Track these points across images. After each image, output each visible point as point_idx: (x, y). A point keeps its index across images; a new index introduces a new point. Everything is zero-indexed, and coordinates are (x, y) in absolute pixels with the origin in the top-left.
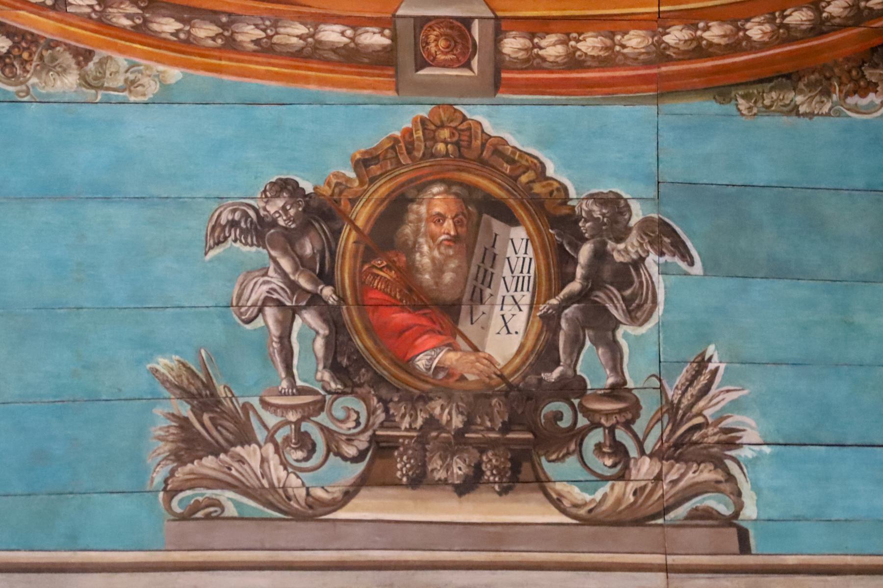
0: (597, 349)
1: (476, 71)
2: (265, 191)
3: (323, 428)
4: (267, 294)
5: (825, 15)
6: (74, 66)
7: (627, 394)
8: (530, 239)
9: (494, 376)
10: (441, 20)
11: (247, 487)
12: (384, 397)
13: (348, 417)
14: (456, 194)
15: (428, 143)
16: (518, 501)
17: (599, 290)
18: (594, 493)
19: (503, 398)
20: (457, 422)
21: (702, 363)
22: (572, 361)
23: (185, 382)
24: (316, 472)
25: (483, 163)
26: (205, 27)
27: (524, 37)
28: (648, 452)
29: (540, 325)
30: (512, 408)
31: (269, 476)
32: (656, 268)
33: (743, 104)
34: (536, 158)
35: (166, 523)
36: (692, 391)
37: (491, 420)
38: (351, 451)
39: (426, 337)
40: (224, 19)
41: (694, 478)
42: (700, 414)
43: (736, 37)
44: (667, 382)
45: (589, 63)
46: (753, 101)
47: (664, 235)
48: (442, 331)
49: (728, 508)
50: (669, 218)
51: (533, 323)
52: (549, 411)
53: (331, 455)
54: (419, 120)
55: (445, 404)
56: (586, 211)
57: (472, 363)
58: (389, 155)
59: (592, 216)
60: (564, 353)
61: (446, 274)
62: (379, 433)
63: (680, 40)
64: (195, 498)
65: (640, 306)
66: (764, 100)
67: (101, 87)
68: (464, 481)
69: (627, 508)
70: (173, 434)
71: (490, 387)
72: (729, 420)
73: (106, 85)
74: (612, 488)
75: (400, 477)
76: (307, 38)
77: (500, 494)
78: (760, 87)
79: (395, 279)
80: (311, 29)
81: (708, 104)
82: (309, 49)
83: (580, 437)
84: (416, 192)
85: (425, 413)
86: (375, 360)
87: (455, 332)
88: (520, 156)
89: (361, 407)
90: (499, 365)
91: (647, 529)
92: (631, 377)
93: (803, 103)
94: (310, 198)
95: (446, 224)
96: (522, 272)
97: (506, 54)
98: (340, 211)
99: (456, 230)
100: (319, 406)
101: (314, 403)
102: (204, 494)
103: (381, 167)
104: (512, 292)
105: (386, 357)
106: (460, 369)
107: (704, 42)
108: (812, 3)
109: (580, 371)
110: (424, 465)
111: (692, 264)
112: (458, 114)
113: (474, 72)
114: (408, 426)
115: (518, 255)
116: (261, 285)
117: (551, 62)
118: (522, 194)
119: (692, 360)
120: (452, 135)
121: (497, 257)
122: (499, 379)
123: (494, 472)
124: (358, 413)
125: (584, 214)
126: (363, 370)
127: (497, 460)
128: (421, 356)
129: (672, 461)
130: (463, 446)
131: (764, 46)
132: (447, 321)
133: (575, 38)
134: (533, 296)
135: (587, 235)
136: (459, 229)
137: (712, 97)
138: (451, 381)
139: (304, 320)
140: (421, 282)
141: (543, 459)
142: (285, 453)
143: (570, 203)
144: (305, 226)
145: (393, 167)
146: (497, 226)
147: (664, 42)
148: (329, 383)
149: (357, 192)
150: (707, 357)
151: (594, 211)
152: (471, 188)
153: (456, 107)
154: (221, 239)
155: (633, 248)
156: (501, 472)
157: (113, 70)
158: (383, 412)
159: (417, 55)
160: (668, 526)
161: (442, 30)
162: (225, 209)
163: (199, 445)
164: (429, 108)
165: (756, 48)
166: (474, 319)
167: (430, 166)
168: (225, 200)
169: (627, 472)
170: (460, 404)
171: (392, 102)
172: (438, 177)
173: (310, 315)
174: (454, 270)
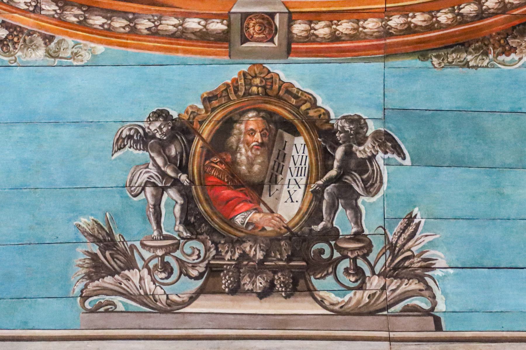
1: (277, 43)
3: (177, 259)
8: (306, 144)
9: (283, 228)
10: (257, 14)
13: (193, 253)
14: (262, 117)
15: (247, 87)
20: (260, 255)
21: (410, 219)
24: (172, 285)
25: (278, 97)
27: (306, 23)
33: (435, 61)
36: (405, 236)
37: (280, 254)
38: (194, 273)
39: (242, 204)
48: (252, 201)
55: (253, 244)
57: (270, 220)
61: (255, 166)
62: (212, 262)
65: (372, 185)
71: (282, 235)
75: (224, 288)
84: (239, 117)
85: (240, 250)
86: (210, 217)
87: (260, 201)
88: (302, 94)
89: (201, 247)
90: (286, 221)
95: (256, 136)
96: (301, 165)
97: (294, 34)
99: (262, 139)
102: (103, 298)
104: (294, 177)
106: (262, 224)
110: (239, 282)
111: (404, 158)
112: (265, 69)
113: (275, 44)
114: (229, 258)
115: (299, 154)
120: (261, 82)
121: (286, 155)
122: (286, 230)
124: (199, 250)
128: (239, 216)
131: (448, 26)
132: (255, 195)
136: (264, 139)
138: (257, 230)
140: (240, 171)
142: (154, 274)
146: (287, 136)
152: (271, 114)
153: (264, 65)
158: (215, 249)
164: (249, 66)
166: (271, 193)
167: (247, 101)
170: (262, 244)
172: (252, 107)
174: (260, 164)
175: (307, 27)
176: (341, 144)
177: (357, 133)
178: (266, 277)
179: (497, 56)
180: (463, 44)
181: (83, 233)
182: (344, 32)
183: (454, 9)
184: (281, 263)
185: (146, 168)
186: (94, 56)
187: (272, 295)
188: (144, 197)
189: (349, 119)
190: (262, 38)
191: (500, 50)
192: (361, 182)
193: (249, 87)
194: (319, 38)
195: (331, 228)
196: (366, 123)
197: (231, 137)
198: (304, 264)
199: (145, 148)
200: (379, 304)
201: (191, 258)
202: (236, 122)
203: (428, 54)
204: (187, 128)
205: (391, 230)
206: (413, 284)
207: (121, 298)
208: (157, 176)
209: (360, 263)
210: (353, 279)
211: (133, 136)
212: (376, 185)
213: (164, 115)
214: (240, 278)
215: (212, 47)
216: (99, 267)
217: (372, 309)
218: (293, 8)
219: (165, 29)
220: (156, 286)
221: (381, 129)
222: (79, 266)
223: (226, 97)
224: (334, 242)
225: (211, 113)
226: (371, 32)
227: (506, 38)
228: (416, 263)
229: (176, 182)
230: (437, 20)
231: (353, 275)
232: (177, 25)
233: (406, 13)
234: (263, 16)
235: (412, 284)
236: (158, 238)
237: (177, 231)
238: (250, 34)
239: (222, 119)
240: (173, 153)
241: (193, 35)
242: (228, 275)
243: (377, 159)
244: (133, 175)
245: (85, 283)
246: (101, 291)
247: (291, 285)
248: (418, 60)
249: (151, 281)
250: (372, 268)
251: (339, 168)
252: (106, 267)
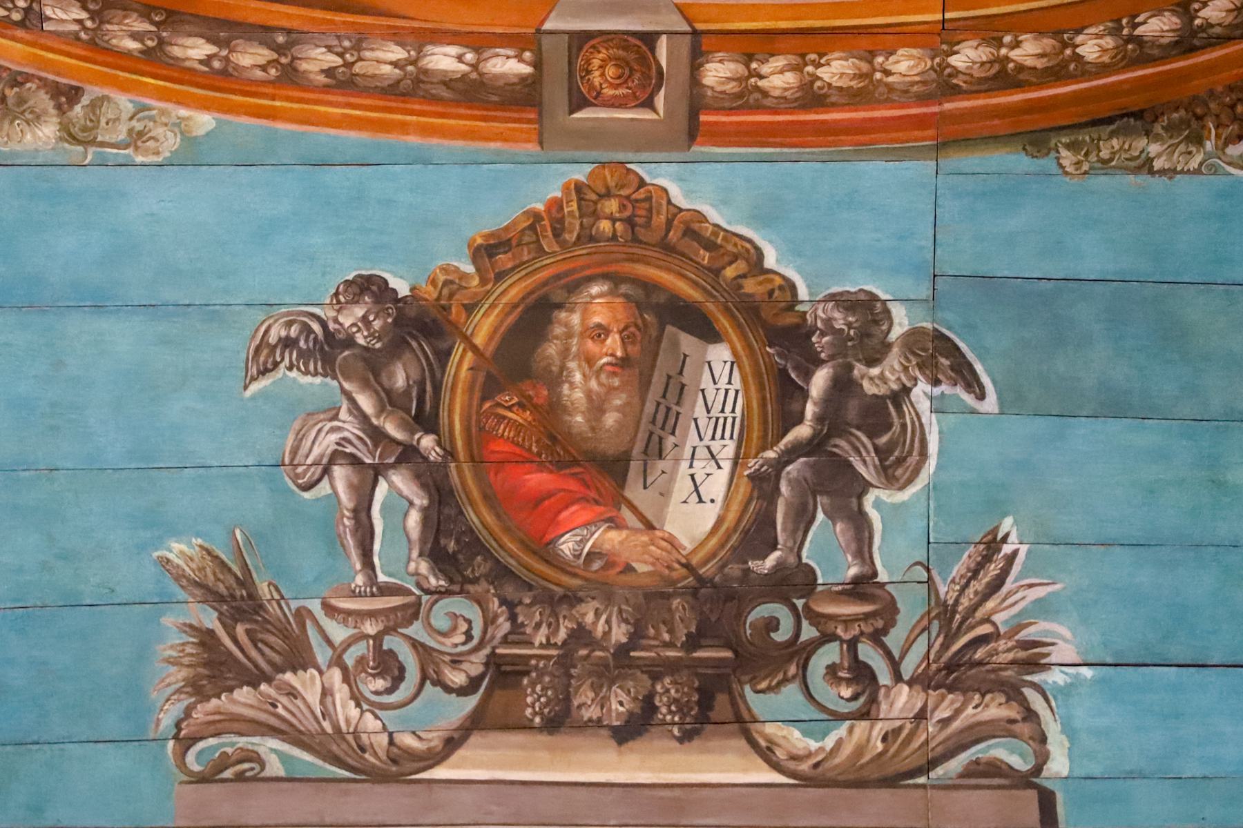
0: (834, 525)
1: (661, 113)
2: (336, 294)
3: (415, 644)
4: (336, 447)
5: (1197, 22)
6: (53, 111)
7: (878, 592)
8: (736, 362)
9: (677, 566)
10: (610, 37)
11: (300, 732)
12: (509, 598)
13: (454, 628)
14: (626, 296)
16: (709, 751)
17: (840, 436)
18: (823, 739)
19: (689, 598)
20: (619, 634)
22: (795, 543)
23: (211, 578)
24: (402, 710)
25: (668, 248)
26: (252, 51)
27: (737, 61)
28: (906, 677)
29: (749, 490)
30: (702, 613)
31: (334, 717)
32: (928, 403)
34: (750, 241)
35: (176, 784)
37: (671, 631)
39: (574, 508)
40: (281, 39)
41: (974, 715)
42: (987, 620)
43: (1061, 57)
44: (939, 574)
45: (833, 99)
46: (1083, 153)
47: (940, 354)
49: (1025, 762)
50: (949, 328)
51: (737, 486)
52: (758, 617)
53: (428, 682)
54: (573, 186)
55: (602, 607)
56: (822, 320)
57: (645, 545)
58: (526, 239)
59: (833, 327)
60: (784, 530)
61: (607, 415)
62: (498, 651)
63: (974, 63)
64: (222, 750)
66: (1100, 151)
67: (93, 142)
68: (627, 722)
69: (872, 760)
70: (192, 655)
71: (673, 583)
72: (1032, 629)
73: (100, 138)
74: (851, 730)
75: (530, 717)
76: (406, 65)
77: (681, 740)
78: (1095, 133)
79: (530, 422)
80: (412, 53)
81: (1013, 157)
82: (409, 82)
83: (804, 656)
87: (619, 500)
88: (725, 239)
89: (474, 613)
91: (900, 791)
92: (884, 566)
93: (1159, 155)
94: (405, 303)
95: (609, 341)
96: (723, 411)
97: (708, 87)
98: (450, 322)
100: (410, 611)
101: (403, 607)
103: (514, 257)
104: (707, 441)
105: (514, 539)
106: (625, 556)
107: (1011, 65)
108: (1178, 5)
109: (807, 557)
110: (568, 699)
112: (632, 176)
113: (658, 114)
114: (544, 641)
115: (717, 386)
116: (327, 433)
117: (776, 98)
118: (726, 295)
119: (977, 541)
120: (622, 207)
122: (684, 571)
123: (673, 708)
124: (469, 622)
125: (819, 324)
126: (479, 558)
127: (677, 691)
128: (567, 536)
129: (943, 691)
130: (627, 670)
132: (607, 484)
133: (814, 61)
134: (739, 447)
135: (823, 355)
136: (630, 348)
137: (1020, 148)
138: (613, 572)
139: (391, 485)
140: (570, 427)
141: (747, 689)
143: (799, 308)
144: (396, 345)
145: (531, 257)
146: (688, 342)
147: (949, 65)
148: (427, 578)
149: (476, 294)
150: (1000, 536)
151: (835, 319)
152: (649, 287)
153: (629, 166)
154: (269, 366)
155: (893, 374)
156: (682, 709)
157: (111, 116)
159: (573, 91)
160: (934, 787)
161: (611, 51)
162: (276, 321)
163: (230, 671)
165: (1090, 73)
166: (649, 482)
167: (587, 254)
168: (275, 307)
169: (874, 707)
170: (624, 607)
171: (532, 160)
173: (400, 478)
174: (618, 409)
175: (740, 69)
176: (823, 362)
177: (864, 335)
178: (635, 687)
179: (1226, 144)
181: (177, 579)
182: (834, 84)
183: (1121, 25)
184: (671, 653)
185: (331, 420)
187: (647, 735)
188: (330, 491)
189: (844, 302)
190: (625, 96)
192: (873, 454)
193: (591, 220)
194: (770, 99)
195: (797, 567)
196: (887, 312)
197: (546, 345)
198: (728, 654)
199: (329, 369)
200: (906, 758)
201: (448, 641)
202: (559, 306)
203: (1049, 140)
204: (434, 321)
205: (944, 571)
206: (993, 705)
207: (274, 743)
208: (360, 438)
209: (867, 653)
210: (847, 692)
211: (296, 341)
212: (909, 460)
213: (374, 288)
214: (571, 690)
215: (494, 119)
216: (222, 664)
217: (891, 770)
218: (705, 22)
219: (371, 71)
220: (362, 712)
221: (924, 324)
222: (169, 662)
223: (532, 246)
224: (803, 601)
225: (494, 285)
226: (904, 83)
228: (1004, 652)
229: (408, 455)
230: (1074, 52)
231: (849, 682)
232: (403, 63)
233: (996, 34)
234: (626, 40)
235: (991, 705)
236: (365, 591)
237: (413, 575)
238: (591, 87)
239: (523, 298)
240: (400, 381)
241: (444, 88)
242: (540, 683)
243: (913, 399)
244: (300, 436)
245: (186, 703)
246: (227, 724)
247: (697, 708)
248: (1023, 154)
249: (351, 698)
250: (895, 666)
251: (819, 419)
252: (236, 660)
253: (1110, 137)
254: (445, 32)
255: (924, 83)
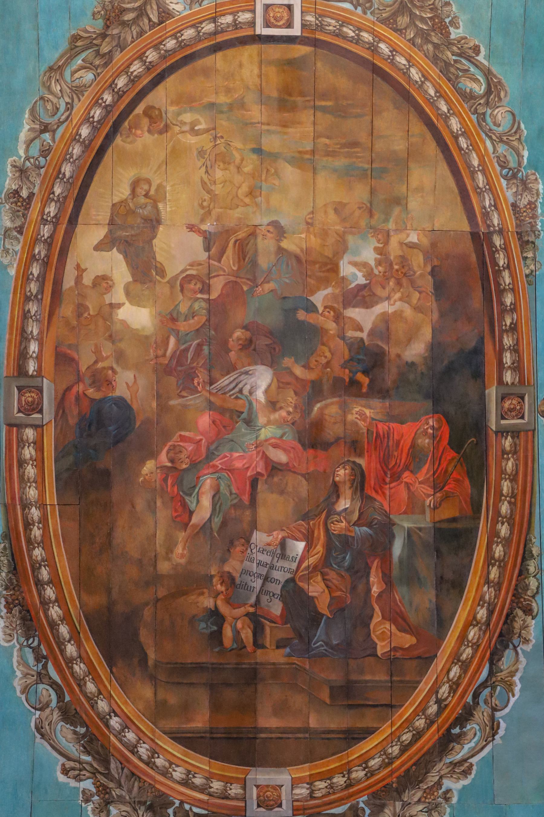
175: (31, 440)
180: (15, 569)
186: (6, 267)
191: (10, 600)
215: (14, 362)
227: (20, 604)
238: (25, 393)
253: (8, 560)
254: (42, 348)
255: (26, 499)
